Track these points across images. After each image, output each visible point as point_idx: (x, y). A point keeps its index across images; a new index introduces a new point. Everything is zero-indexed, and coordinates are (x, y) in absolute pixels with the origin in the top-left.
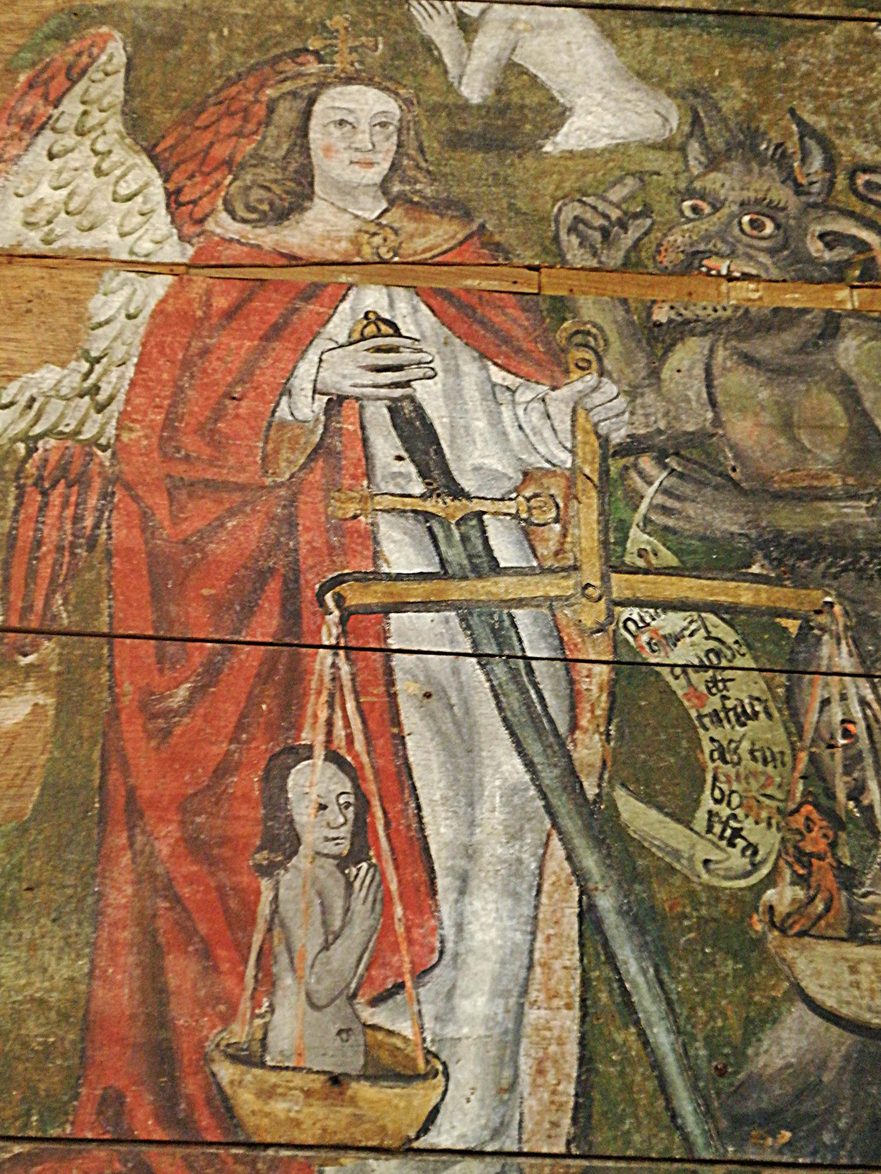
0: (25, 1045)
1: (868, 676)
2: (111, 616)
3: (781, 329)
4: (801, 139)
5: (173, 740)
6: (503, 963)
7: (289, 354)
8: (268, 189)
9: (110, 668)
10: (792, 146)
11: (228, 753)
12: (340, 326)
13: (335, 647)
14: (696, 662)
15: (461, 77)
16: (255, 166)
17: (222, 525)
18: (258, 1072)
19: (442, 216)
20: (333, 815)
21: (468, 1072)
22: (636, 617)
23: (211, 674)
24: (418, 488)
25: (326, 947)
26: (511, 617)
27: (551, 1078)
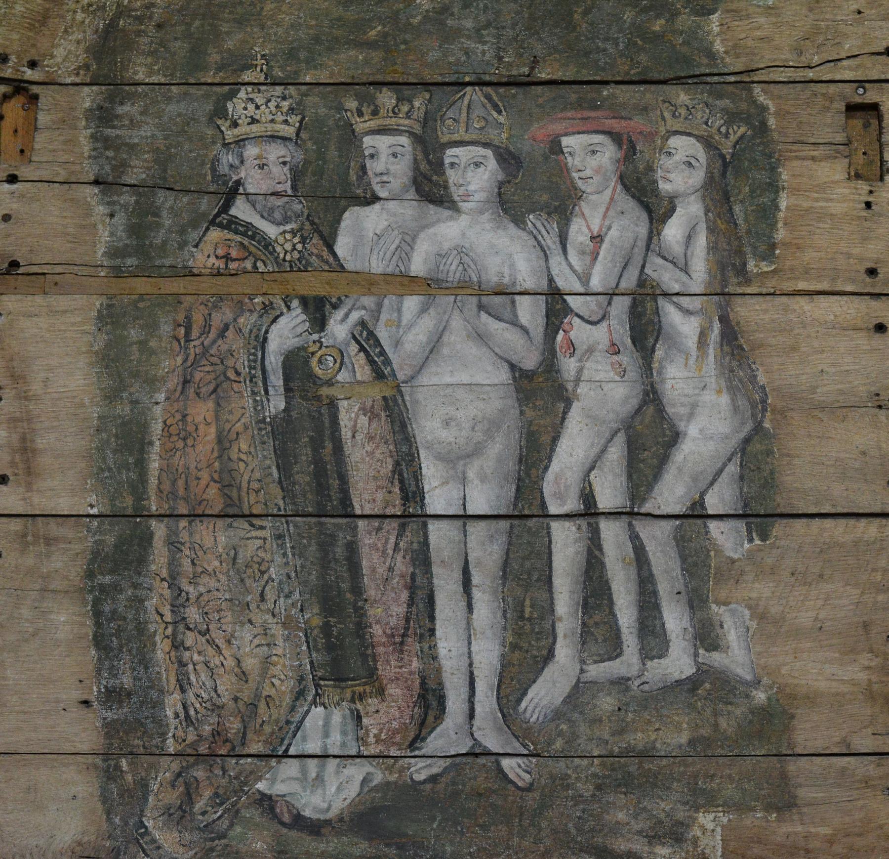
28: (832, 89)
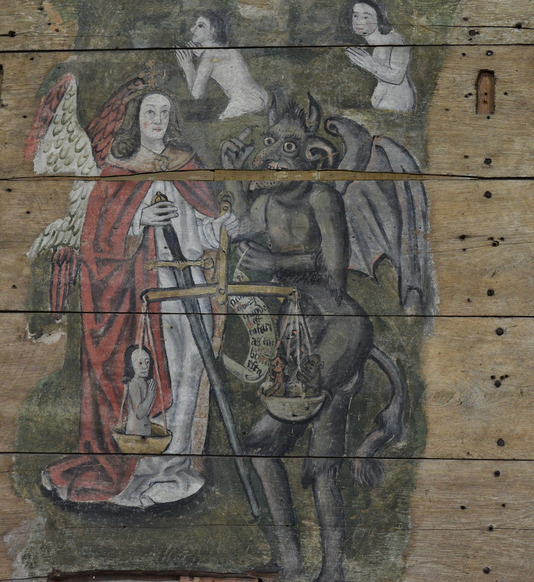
0: (65, 430)
1: (303, 315)
3: (292, 190)
4: (310, 107)
5: (101, 344)
6: (188, 406)
7: (132, 211)
8: (125, 143)
9: (82, 323)
10: (307, 111)
11: (115, 348)
12: (148, 199)
13: (146, 313)
16: (121, 134)
17: (113, 274)
18: (124, 436)
19: (183, 150)
20: (144, 366)
21: (178, 435)
23: (110, 323)
24: (171, 258)
25: (142, 403)
26: (197, 301)
27: (199, 436)
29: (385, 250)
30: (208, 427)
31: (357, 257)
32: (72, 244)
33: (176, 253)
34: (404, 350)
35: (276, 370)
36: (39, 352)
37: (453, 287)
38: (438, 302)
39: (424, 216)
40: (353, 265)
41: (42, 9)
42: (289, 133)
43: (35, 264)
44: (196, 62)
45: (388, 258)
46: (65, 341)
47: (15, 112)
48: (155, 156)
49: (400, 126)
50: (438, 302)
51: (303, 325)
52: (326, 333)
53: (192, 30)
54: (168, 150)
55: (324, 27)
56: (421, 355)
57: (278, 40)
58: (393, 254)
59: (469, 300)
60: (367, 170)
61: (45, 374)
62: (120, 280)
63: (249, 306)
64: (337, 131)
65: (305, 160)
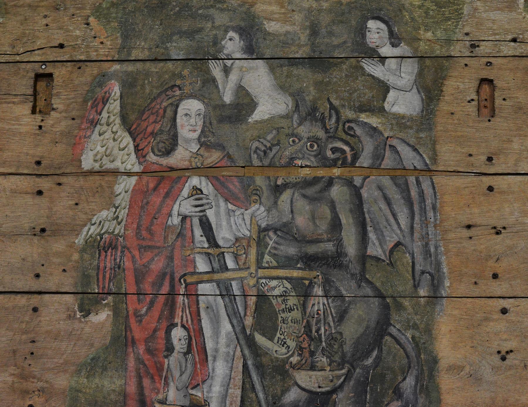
0: (111, 401)
1: (326, 296)
2: (125, 289)
4: (330, 111)
6: (224, 378)
7: (171, 203)
8: (164, 143)
9: (126, 303)
10: (327, 114)
11: (157, 326)
12: (185, 192)
14: (280, 294)
15: (224, 93)
16: (160, 134)
17: (154, 259)
19: (216, 149)
20: (183, 342)
22: (264, 282)
23: (152, 304)
24: (206, 245)
25: (181, 375)
26: (231, 284)
28: (29, 66)
29: (400, 238)
30: (242, 397)
31: (374, 244)
32: (116, 232)
33: (211, 240)
34: (418, 328)
35: (303, 346)
36: (87, 329)
37: (461, 271)
38: (448, 285)
39: (434, 208)
40: (371, 251)
41: (88, 24)
42: (311, 134)
43: (83, 250)
44: (227, 71)
45: (403, 245)
46: (111, 320)
47: (64, 114)
48: (191, 154)
49: (411, 128)
50: (448, 285)
51: (327, 305)
52: (347, 312)
53: (223, 43)
54: (203, 149)
55: (341, 40)
56: (433, 332)
57: (300, 52)
58: (407, 241)
59: (476, 283)
60: (382, 167)
61: (93, 349)
62: (161, 265)
63: (278, 288)
64: (355, 133)
65: (325, 158)
